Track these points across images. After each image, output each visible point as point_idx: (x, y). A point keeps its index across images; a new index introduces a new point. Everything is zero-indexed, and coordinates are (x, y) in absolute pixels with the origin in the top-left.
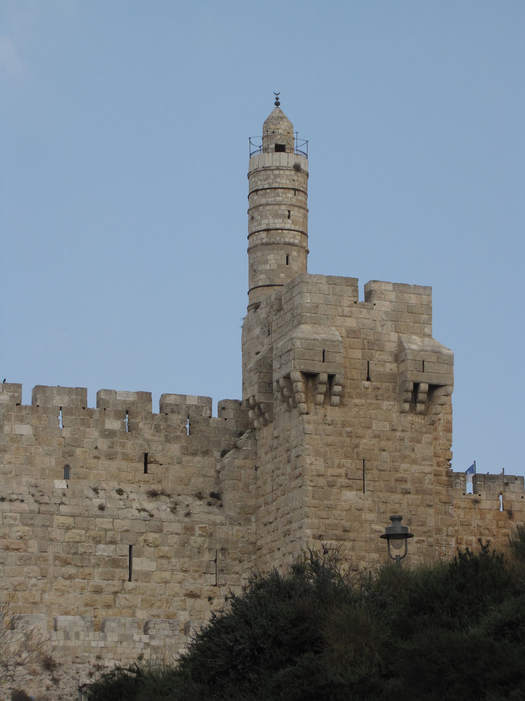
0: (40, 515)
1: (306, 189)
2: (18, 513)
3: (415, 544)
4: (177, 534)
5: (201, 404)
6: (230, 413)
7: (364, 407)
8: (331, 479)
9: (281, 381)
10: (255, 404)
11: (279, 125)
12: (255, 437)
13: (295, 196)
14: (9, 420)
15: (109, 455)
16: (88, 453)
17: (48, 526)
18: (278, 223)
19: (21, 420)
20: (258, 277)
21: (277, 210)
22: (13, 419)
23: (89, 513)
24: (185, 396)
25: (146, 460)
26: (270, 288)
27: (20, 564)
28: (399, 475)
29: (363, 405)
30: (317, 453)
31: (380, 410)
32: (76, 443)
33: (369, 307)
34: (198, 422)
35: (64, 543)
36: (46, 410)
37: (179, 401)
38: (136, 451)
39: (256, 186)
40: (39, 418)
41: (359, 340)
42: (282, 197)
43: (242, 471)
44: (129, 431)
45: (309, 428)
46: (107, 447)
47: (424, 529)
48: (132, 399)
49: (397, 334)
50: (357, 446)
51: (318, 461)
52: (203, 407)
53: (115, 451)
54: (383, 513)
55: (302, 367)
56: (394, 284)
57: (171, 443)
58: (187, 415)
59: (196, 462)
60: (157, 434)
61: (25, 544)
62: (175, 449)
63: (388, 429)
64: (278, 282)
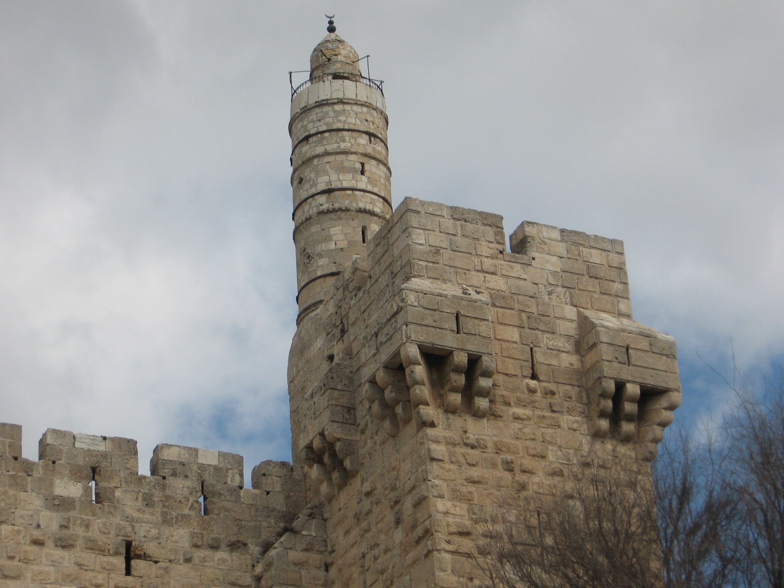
5: (223, 465)
6: (275, 483)
7: (532, 422)
9: (381, 376)
12: (322, 516)
13: (370, 143)
15: (60, 539)
16: (22, 535)
18: (347, 180)
20: (315, 265)
21: (342, 162)
25: (130, 553)
29: (529, 419)
31: (559, 430)
34: (220, 495)
37: (185, 457)
41: (512, 312)
42: (350, 142)
43: (303, 572)
44: (97, 502)
45: (439, 450)
46: (58, 527)
48: (102, 447)
49: (575, 309)
50: (523, 487)
51: (458, 509)
52: (227, 469)
53: (73, 535)
56: (562, 231)
57: (172, 526)
59: (219, 560)
60: (147, 510)
62: (181, 536)
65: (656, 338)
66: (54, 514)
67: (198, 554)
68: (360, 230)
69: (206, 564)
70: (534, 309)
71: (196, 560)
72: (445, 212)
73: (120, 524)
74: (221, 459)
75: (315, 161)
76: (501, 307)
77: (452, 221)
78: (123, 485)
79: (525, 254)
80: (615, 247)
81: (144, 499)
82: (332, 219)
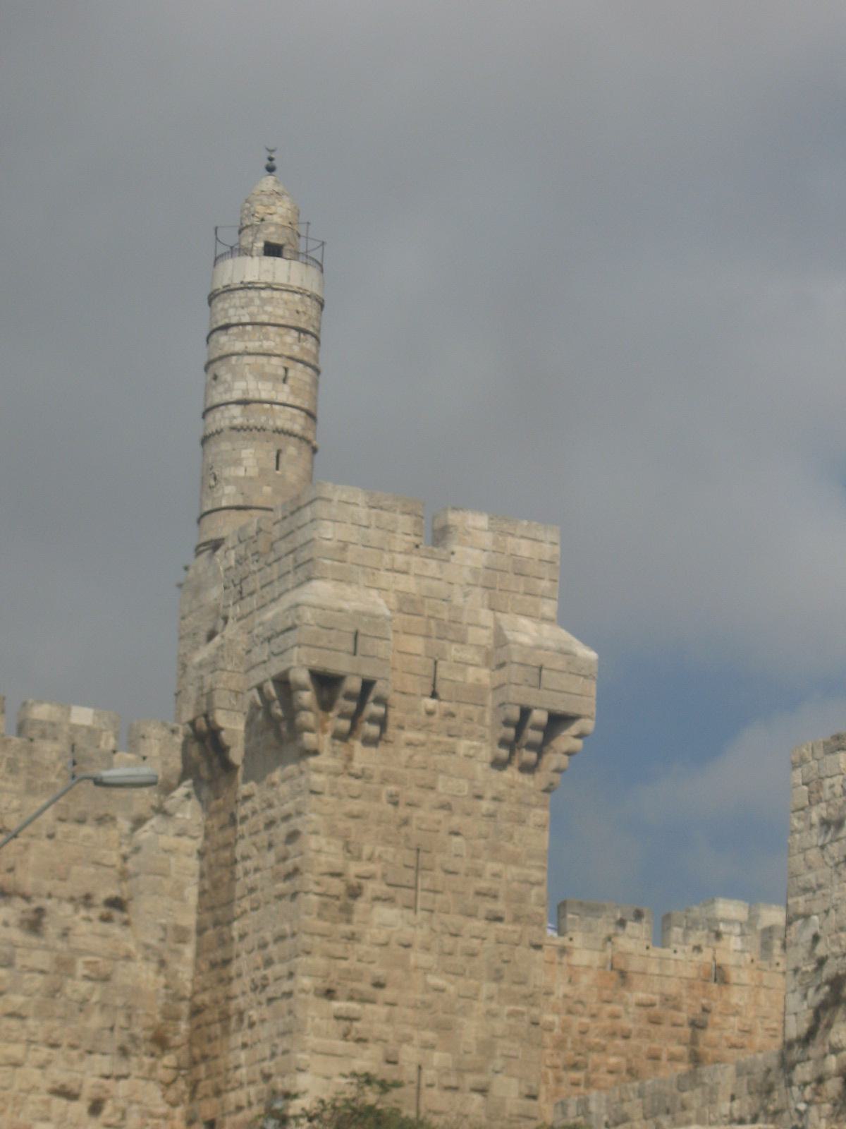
1: (319, 331)
3: (505, 1018)
4: (42, 972)
8: (354, 881)
11: (273, 207)
18: (265, 391)
20: (221, 492)
21: (263, 366)
26: (243, 512)
28: (483, 884)
29: (423, 744)
30: (333, 832)
39: (226, 316)
43: (173, 860)
47: (524, 990)
49: (491, 613)
50: (406, 822)
52: (102, 731)
54: (450, 954)
55: (314, 662)
63: (466, 793)
64: (257, 500)
65: (575, 655)
68: (274, 454)
69: (71, 840)
70: (445, 616)
71: (59, 836)
75: (234, 359)
81: (8, 765)
82: (244, 439)
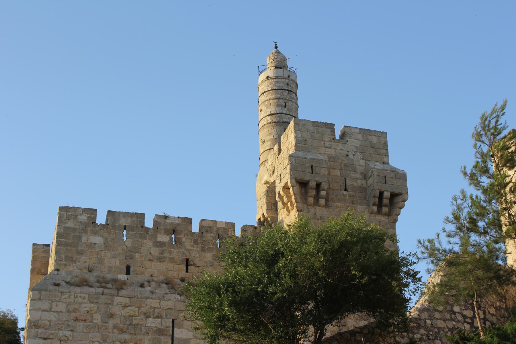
0: (104, 296)
2: (87, 294)
6: (249, 235)
10: (265, 220)
14: (86, 233)
16: (144, 257)
17: (110, 304)
19: (95, 233)
22: (89, 232)
23: (142, 296)
24: (216, 221)
25: (187, 263)
27: (86, 331)
32: (136, 250)
33: (344, 143)
35: (121, 317)
36: (114, 227)
37: (211, 224)
38: (180, 257)
40: (109, 233)
41: (337, 163)
48: (177, 221)
49: (364, 161)
52: (229, 229)
56: (361, 129)
57: (205, 252)
58: (217, 234)
60: (195, 246)
61: (91, 317)
62: (209, 256)
66: (157, 249)
67: (216, 263)
72: (310, 124)
73: (184, 252)
74: (226, 225)
76: (333, 162)
77: (313, 127)
78: (186, 236)
79: (344, 139)
80: (384, 134)
81: (194, 242)
